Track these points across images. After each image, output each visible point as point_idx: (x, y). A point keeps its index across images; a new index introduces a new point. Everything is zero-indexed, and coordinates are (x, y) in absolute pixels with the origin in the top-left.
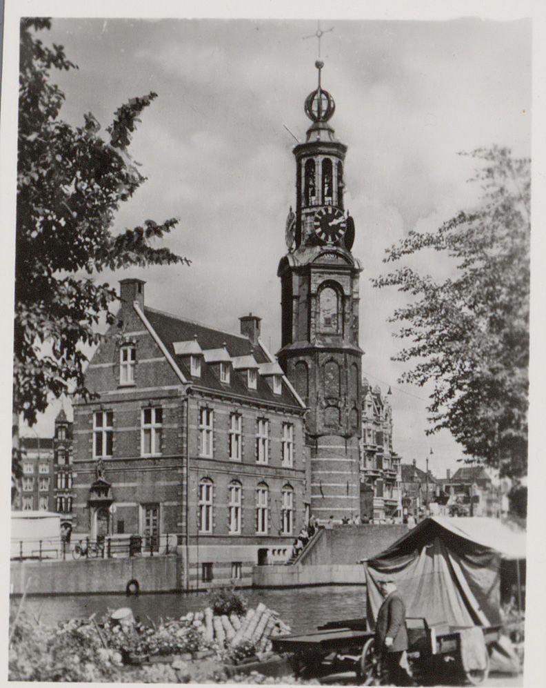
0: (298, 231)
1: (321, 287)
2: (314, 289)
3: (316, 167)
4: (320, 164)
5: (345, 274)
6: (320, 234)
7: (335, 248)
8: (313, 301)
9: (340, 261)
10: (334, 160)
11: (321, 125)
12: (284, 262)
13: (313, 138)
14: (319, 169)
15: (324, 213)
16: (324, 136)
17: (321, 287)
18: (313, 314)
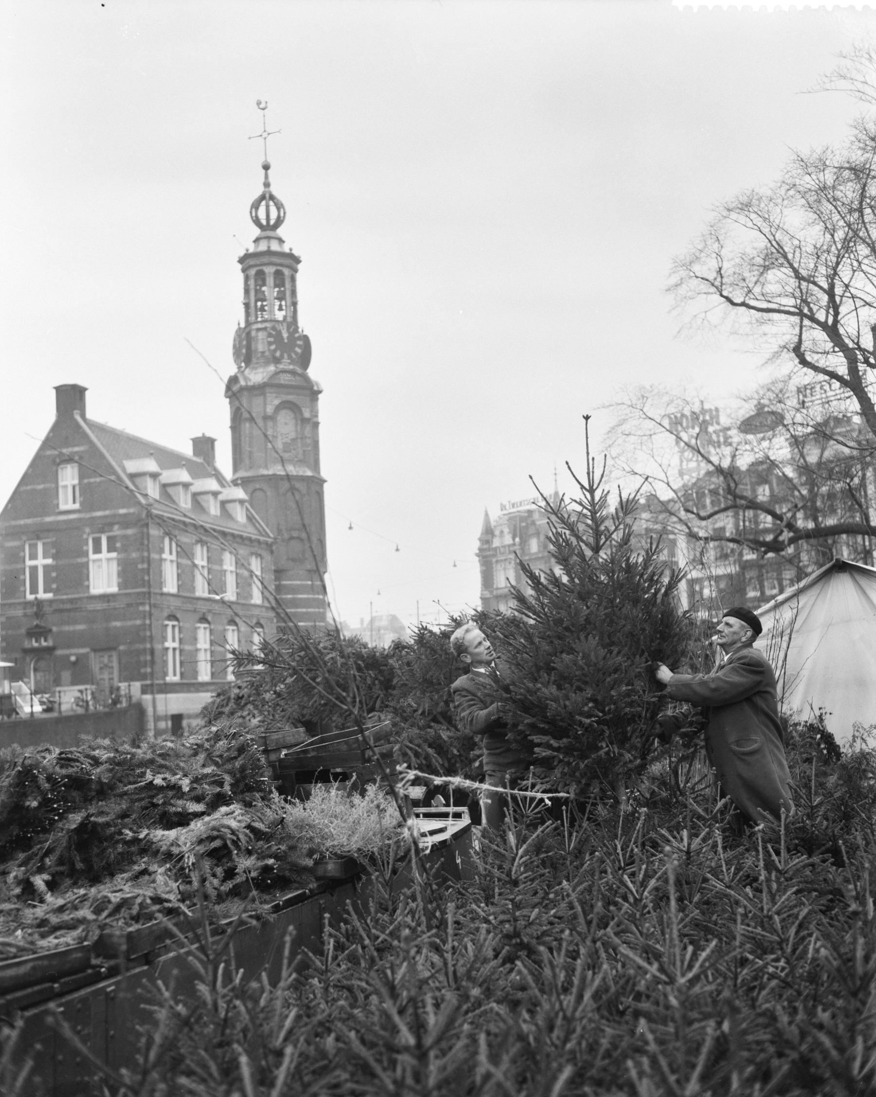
0: (249, 347)
2: (270, 410)
6: (275, 351)
7: (291, 367)
10: (287, 272)
11: (269, 233)
12: (233, 380)
13: (263, 247)
14: (270, 280)
16: (275, 247)
17: (278, 409)
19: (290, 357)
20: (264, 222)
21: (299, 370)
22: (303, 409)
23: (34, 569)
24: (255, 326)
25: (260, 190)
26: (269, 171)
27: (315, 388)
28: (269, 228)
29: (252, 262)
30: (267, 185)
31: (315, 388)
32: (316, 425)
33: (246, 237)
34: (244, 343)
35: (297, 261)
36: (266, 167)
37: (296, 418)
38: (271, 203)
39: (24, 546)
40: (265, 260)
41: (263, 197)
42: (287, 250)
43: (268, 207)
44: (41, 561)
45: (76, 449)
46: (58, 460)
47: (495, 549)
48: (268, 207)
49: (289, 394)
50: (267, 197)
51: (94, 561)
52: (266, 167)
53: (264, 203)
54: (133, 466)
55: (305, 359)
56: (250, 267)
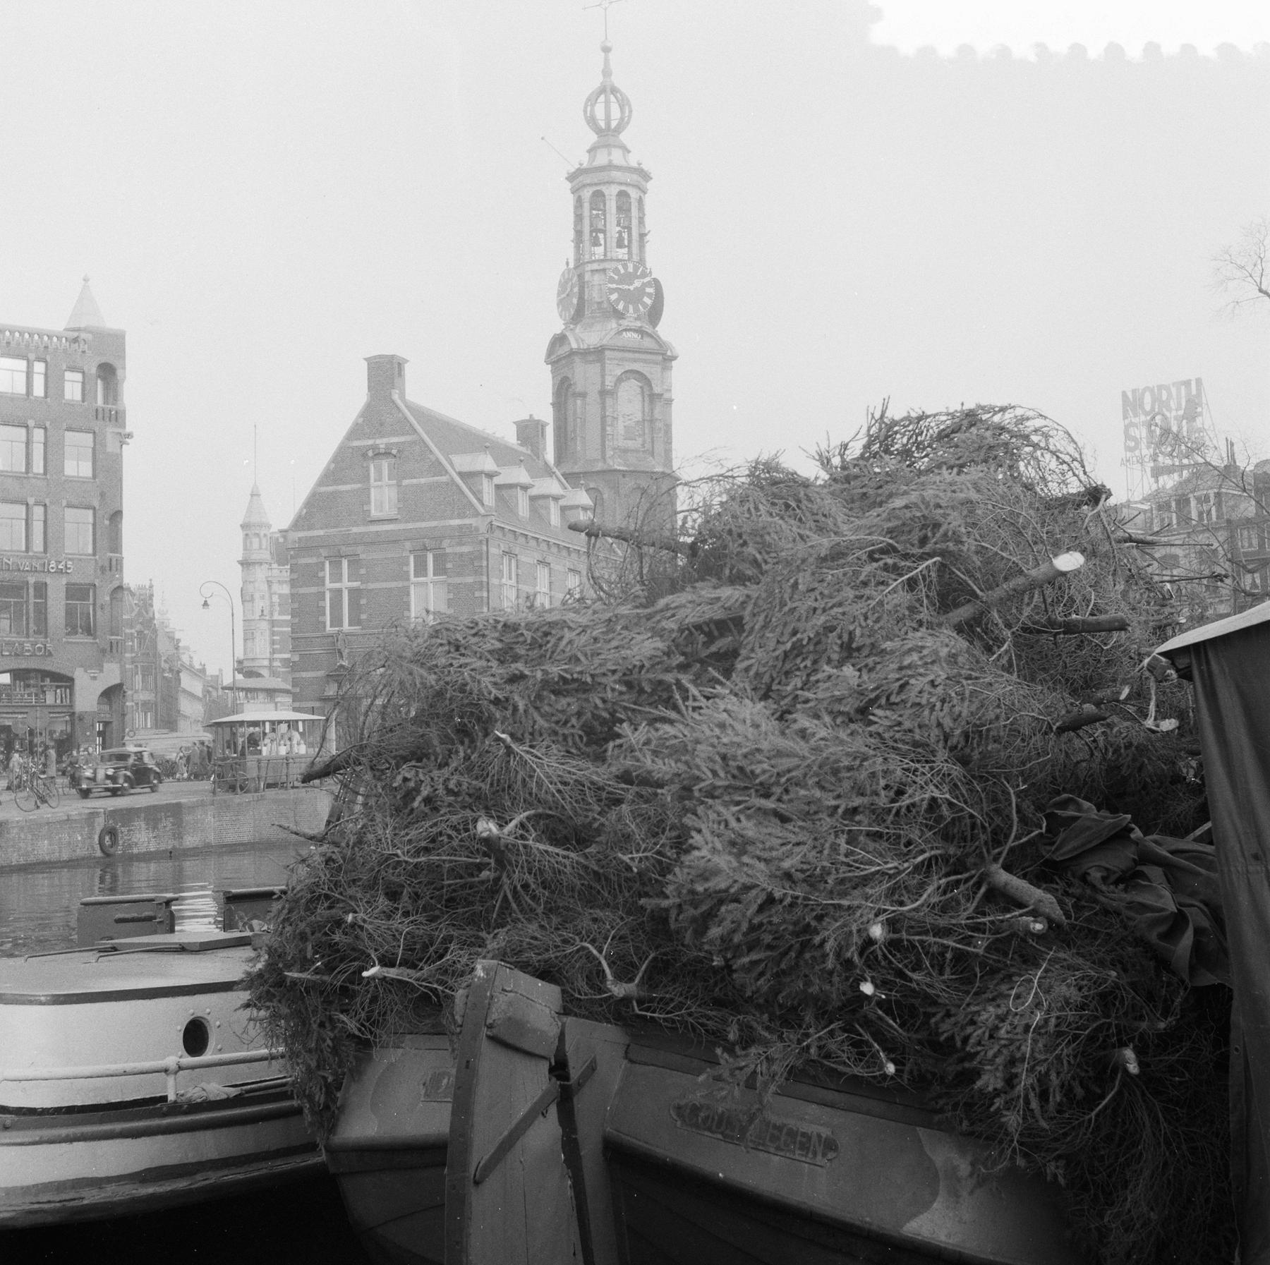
1: (619, 380)
2: (609, 382)
3: (608, 203)
4: (614, 198)
6: (618, 301)
7: (638, 324)
9: (648, 343)
10: (634, 194)
12: (559, 340)
13: (602, 159)
14: (612, 205)
15: (622, 271)
16: (617, 157)
18: (609, 420)
19: (636, 310)
20: (602, 124)
23: (339, 592)
24: (589, 267)
25: (596, 82)
26: (611, 55)
27: (669, 353)
28: (607, 135)
29: (588, 179)
30: (607, 72)
31: (669, 353)
32: (669, 402)
33: (577, 146)
34: (576, 290)
35: (646, 176)
36: (606, 50)
38: (612, 98)
39: (323, 564)
40: (603, 176)
41: (602, 90)
42: (634, 164)
43: (607, 103)
44: (346, 584)
45: (394, 440)
46: (370, 453)
48: (607, 103)
49: (635, 361)
50: (608, 90)
51: (416, 584)
52: (606, 50)
53: (602, 98)
54: (464, 462)
55: (655, 314)
56: (584, 186)
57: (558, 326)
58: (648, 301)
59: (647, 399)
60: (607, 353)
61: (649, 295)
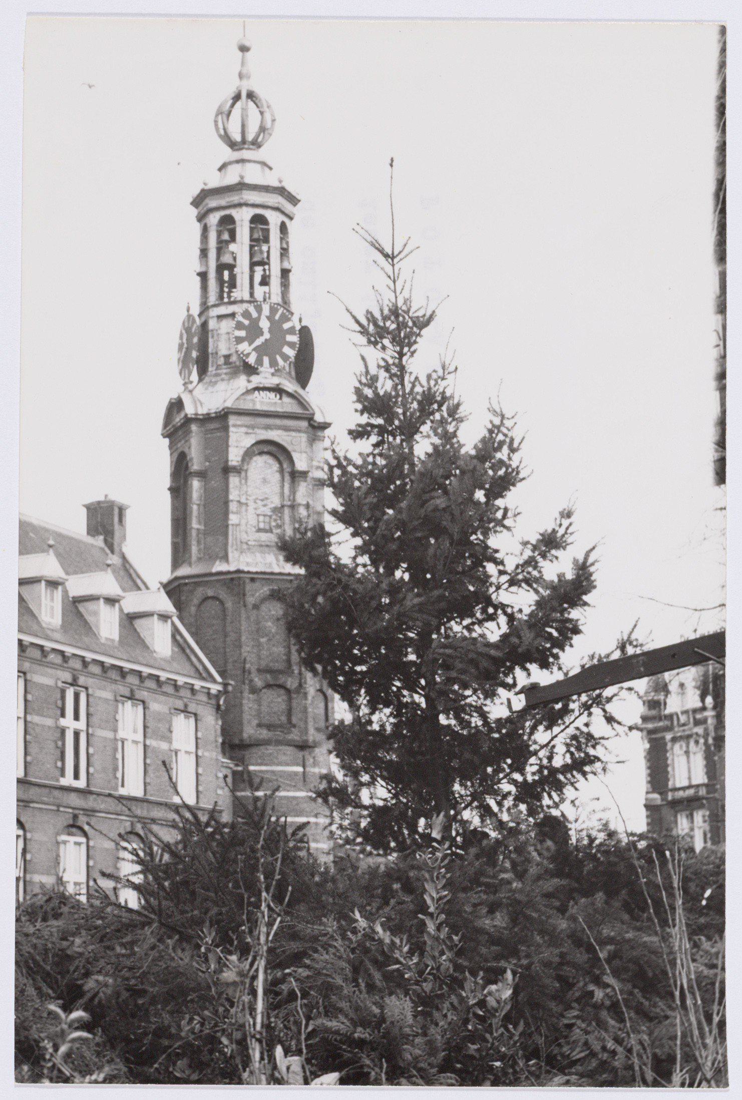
0: (203, 346)
5: (299, 431)
8: (234, 480)
9: (287, 405)
10: (274, 219)
11: (245, 154)
12: (176, 405)
13: (231, 177)
16: (253, 175)
17: (249, 454)
18: (233, 507)
20: (237, 137)
21: (291, 386)
22: (295, 456)
29: (212, 203)
37: (281, 471)
38: (251, 103)
40: (235, 198)
41: (237, 98)
47: (670, 717)
48: (244, 110)
49: (268, 427)
53: (239, 105)
57: (174, 388)
58: (291, 353)
59: (287, 478)
60: (232, 420)
61: (291, 345)
